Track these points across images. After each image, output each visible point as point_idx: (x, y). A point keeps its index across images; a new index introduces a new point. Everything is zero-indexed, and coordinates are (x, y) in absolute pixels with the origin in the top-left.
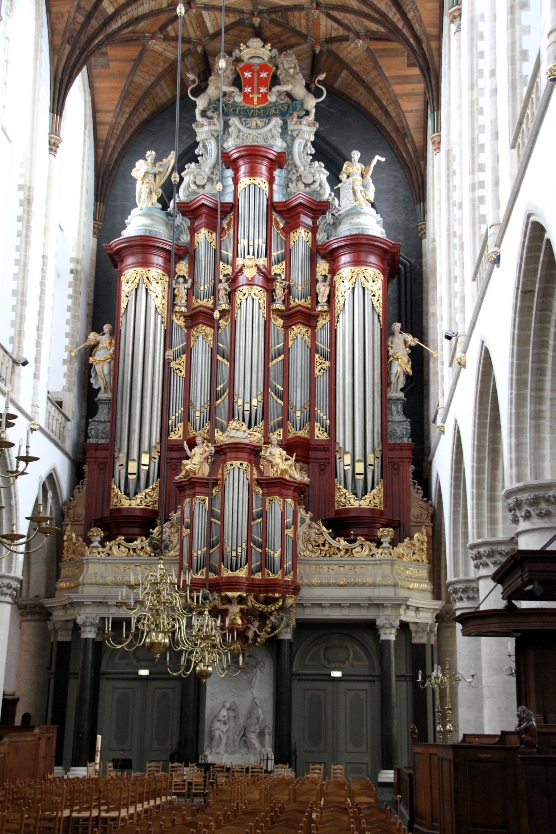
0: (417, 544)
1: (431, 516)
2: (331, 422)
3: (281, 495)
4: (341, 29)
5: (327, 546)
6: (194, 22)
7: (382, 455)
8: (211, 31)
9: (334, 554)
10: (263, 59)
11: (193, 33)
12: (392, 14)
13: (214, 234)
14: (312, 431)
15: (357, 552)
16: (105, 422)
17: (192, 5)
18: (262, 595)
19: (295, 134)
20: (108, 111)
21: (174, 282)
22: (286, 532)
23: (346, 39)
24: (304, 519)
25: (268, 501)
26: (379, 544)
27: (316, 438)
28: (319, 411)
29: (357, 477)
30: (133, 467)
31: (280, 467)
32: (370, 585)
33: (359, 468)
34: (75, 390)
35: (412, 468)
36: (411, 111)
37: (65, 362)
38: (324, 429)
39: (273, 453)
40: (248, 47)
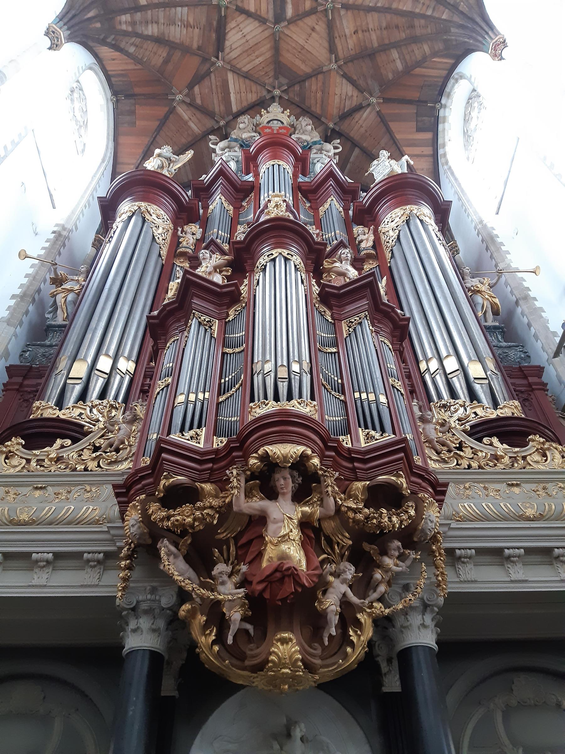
4: (356, 93)
5: (468, 453)
6: (219, 90)
8: (235, 109)
10: (282, 123)
11: (218, 107)
12: (420, 6)
13: (231, 208)
16: (51, 346)
17: (220, 53)
18: (359, 485)
19: (315, 161)
20: (129, 164)
21: (180, 229)
23: (359, 108)
30: (80, 369)
34: (22, 331)
36: (423, 170)
37: (13, 297)
40: (268, 112)
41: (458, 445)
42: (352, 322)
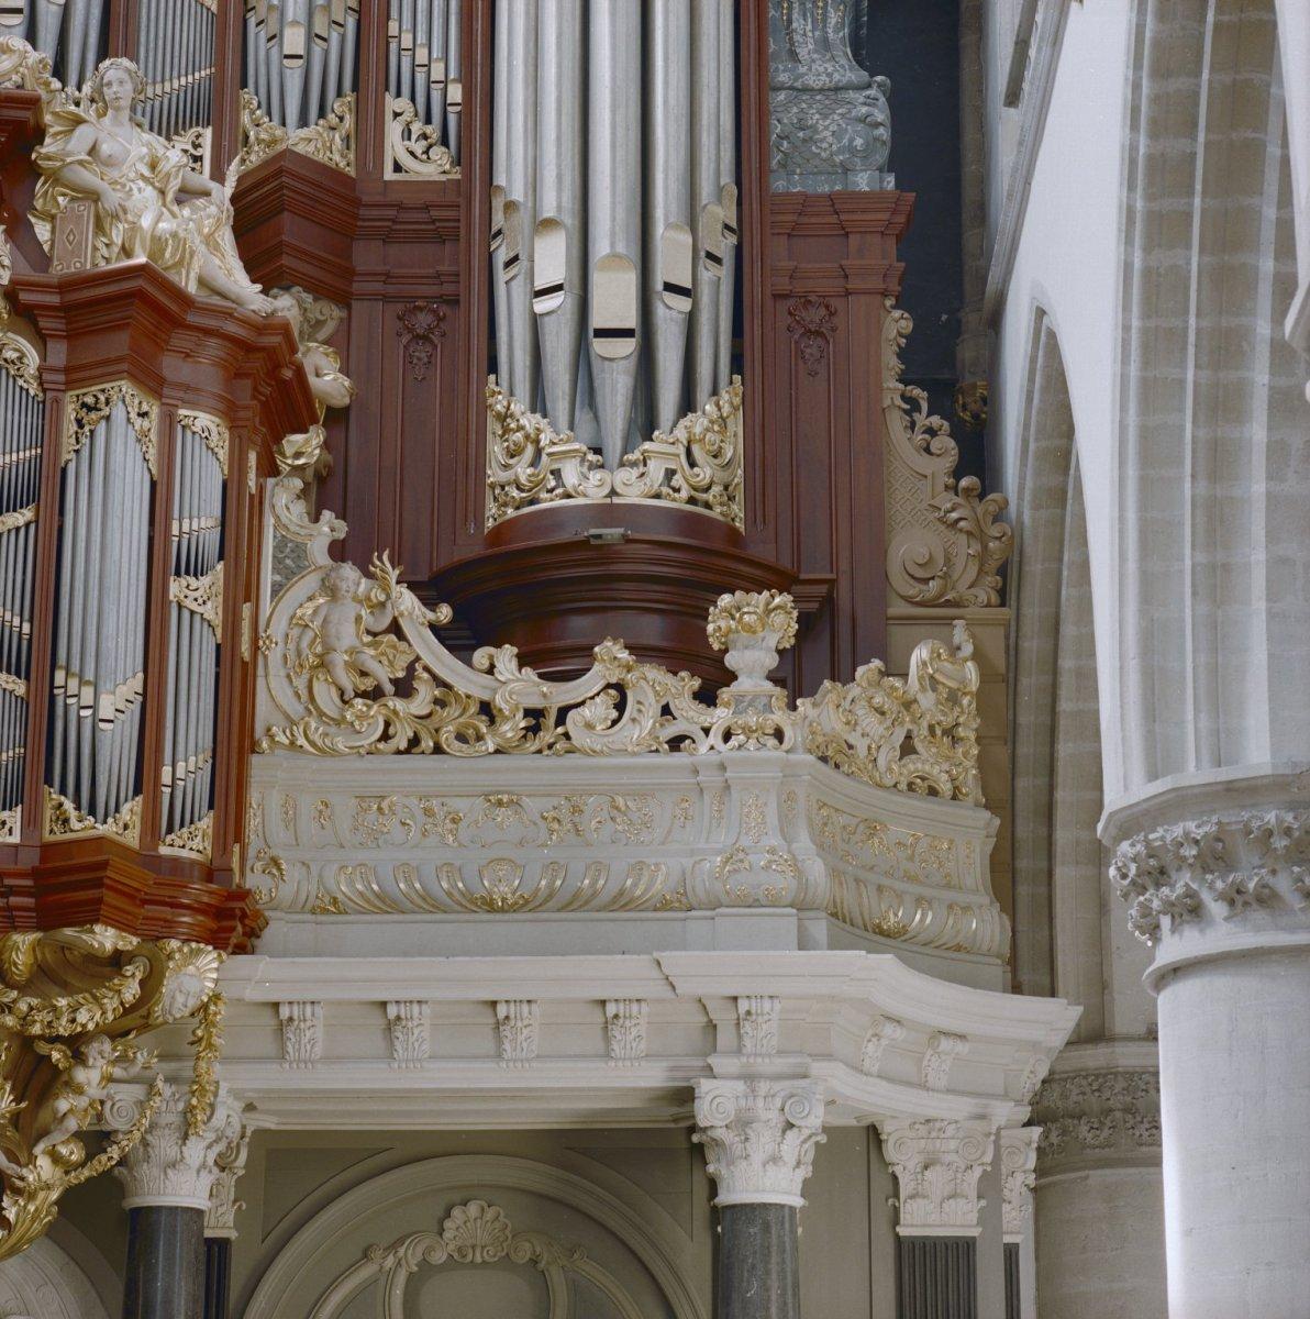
0: (927, 701)
1: (1003, 571)
2: (468, 93)
3: (153, 383)
5: (425, 693)
7: (739, 249)
9: (461, 738)
14: (367, 136)
15: (590, 726)
22: (176, 588)
24: (300, 552)
25: (70, 411)
26: (713, 681)
27: (389, 175)
28: (407, 41)
29: (600, 346)
31: (146, 222)
32: (665, 905)
33: (615, 301)
35: (898, 324)
38: (433, 131)
39: (105, 149)
41: (401, 674)
42: (90, 409)
